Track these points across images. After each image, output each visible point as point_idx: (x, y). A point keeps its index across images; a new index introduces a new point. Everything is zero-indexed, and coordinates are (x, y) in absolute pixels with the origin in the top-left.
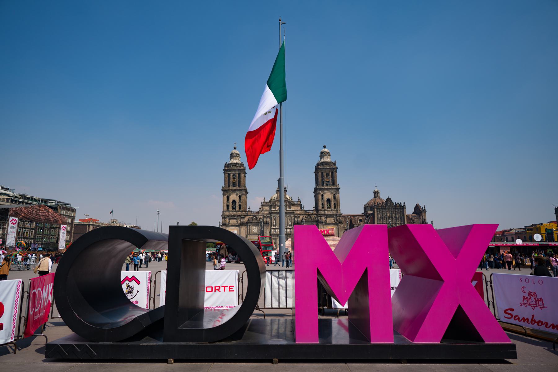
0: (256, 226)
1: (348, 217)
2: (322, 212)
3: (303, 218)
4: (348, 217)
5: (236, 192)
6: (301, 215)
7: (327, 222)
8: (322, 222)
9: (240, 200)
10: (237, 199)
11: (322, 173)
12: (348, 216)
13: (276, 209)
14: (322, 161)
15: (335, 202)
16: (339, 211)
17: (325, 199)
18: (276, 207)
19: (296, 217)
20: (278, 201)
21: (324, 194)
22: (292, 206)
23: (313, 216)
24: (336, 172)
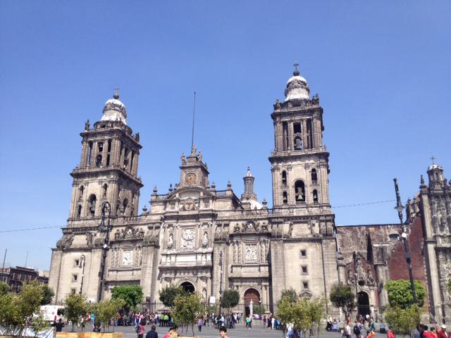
0: (130, 249)
1: (360, 228)
2: (285, 213)
3: (237, 228)
4: (360, 228)
6: (231, 220)
7: (294, 236)
8: (281, 236)
10: (99, 194)
11: (285, 124)
12: (360, 226)
13: (176, 209)
16: (325, 208)
18: (177, 203)
19: (219, 225)
20: (180, 190)
21: (288, 169)
22: (211, 201)
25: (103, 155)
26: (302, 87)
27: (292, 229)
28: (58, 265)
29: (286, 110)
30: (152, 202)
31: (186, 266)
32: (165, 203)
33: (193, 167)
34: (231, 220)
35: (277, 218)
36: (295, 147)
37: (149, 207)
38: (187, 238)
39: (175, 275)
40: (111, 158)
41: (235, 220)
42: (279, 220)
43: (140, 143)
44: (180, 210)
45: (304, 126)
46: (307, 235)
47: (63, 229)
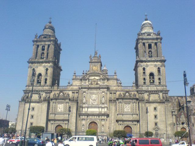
0: (62, 103)
2: (144, 88)
3: (120, 95)
5: (43, 64)
6: (117, 91)
7: (151, 99)
9: (46, 73)
10: (43, 73)
11: (144, 44)
12: (174, 97)
13: (87, 84)
14: (143, 32)
15: (160, 77)
16: (164, 87)
17: (148, 72)
22: (106, 80)
23: (133, 93)
24: (161, 43)
25: (45, 53)
26: (151, 27)
27: (150, 97)
28: (23, 110)
29: (144, 37)
30: (73, 79)
31: (93, 113)
32: (81, 80)
33: (96, 62)
34: (117, 91)
35: (141, 91)
36: (149, 56)
37: (71, 82)
38: (93, 99)
39: (87, 117)
40: (49, 54)
41: (119, 91)
42: (142, 92)
43: (61, 47)
44: (90, 84)
45: (153, 45)
46: (157, 100)
47: (24, 91)
